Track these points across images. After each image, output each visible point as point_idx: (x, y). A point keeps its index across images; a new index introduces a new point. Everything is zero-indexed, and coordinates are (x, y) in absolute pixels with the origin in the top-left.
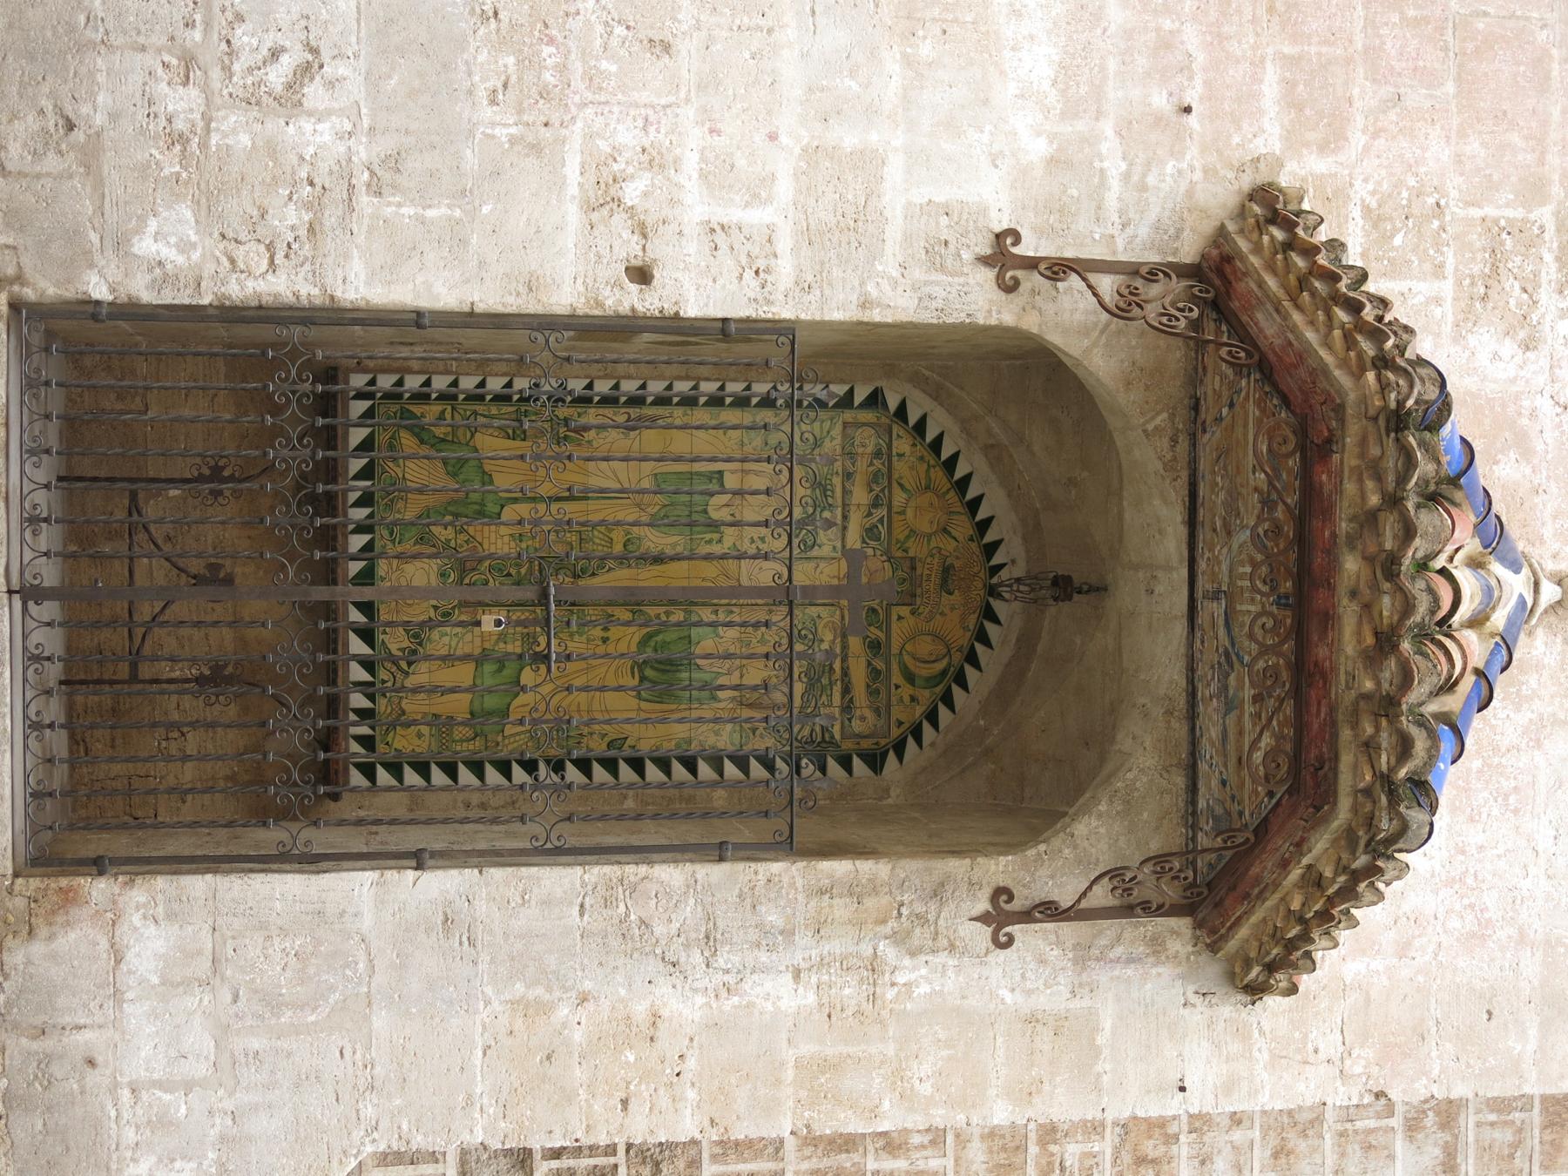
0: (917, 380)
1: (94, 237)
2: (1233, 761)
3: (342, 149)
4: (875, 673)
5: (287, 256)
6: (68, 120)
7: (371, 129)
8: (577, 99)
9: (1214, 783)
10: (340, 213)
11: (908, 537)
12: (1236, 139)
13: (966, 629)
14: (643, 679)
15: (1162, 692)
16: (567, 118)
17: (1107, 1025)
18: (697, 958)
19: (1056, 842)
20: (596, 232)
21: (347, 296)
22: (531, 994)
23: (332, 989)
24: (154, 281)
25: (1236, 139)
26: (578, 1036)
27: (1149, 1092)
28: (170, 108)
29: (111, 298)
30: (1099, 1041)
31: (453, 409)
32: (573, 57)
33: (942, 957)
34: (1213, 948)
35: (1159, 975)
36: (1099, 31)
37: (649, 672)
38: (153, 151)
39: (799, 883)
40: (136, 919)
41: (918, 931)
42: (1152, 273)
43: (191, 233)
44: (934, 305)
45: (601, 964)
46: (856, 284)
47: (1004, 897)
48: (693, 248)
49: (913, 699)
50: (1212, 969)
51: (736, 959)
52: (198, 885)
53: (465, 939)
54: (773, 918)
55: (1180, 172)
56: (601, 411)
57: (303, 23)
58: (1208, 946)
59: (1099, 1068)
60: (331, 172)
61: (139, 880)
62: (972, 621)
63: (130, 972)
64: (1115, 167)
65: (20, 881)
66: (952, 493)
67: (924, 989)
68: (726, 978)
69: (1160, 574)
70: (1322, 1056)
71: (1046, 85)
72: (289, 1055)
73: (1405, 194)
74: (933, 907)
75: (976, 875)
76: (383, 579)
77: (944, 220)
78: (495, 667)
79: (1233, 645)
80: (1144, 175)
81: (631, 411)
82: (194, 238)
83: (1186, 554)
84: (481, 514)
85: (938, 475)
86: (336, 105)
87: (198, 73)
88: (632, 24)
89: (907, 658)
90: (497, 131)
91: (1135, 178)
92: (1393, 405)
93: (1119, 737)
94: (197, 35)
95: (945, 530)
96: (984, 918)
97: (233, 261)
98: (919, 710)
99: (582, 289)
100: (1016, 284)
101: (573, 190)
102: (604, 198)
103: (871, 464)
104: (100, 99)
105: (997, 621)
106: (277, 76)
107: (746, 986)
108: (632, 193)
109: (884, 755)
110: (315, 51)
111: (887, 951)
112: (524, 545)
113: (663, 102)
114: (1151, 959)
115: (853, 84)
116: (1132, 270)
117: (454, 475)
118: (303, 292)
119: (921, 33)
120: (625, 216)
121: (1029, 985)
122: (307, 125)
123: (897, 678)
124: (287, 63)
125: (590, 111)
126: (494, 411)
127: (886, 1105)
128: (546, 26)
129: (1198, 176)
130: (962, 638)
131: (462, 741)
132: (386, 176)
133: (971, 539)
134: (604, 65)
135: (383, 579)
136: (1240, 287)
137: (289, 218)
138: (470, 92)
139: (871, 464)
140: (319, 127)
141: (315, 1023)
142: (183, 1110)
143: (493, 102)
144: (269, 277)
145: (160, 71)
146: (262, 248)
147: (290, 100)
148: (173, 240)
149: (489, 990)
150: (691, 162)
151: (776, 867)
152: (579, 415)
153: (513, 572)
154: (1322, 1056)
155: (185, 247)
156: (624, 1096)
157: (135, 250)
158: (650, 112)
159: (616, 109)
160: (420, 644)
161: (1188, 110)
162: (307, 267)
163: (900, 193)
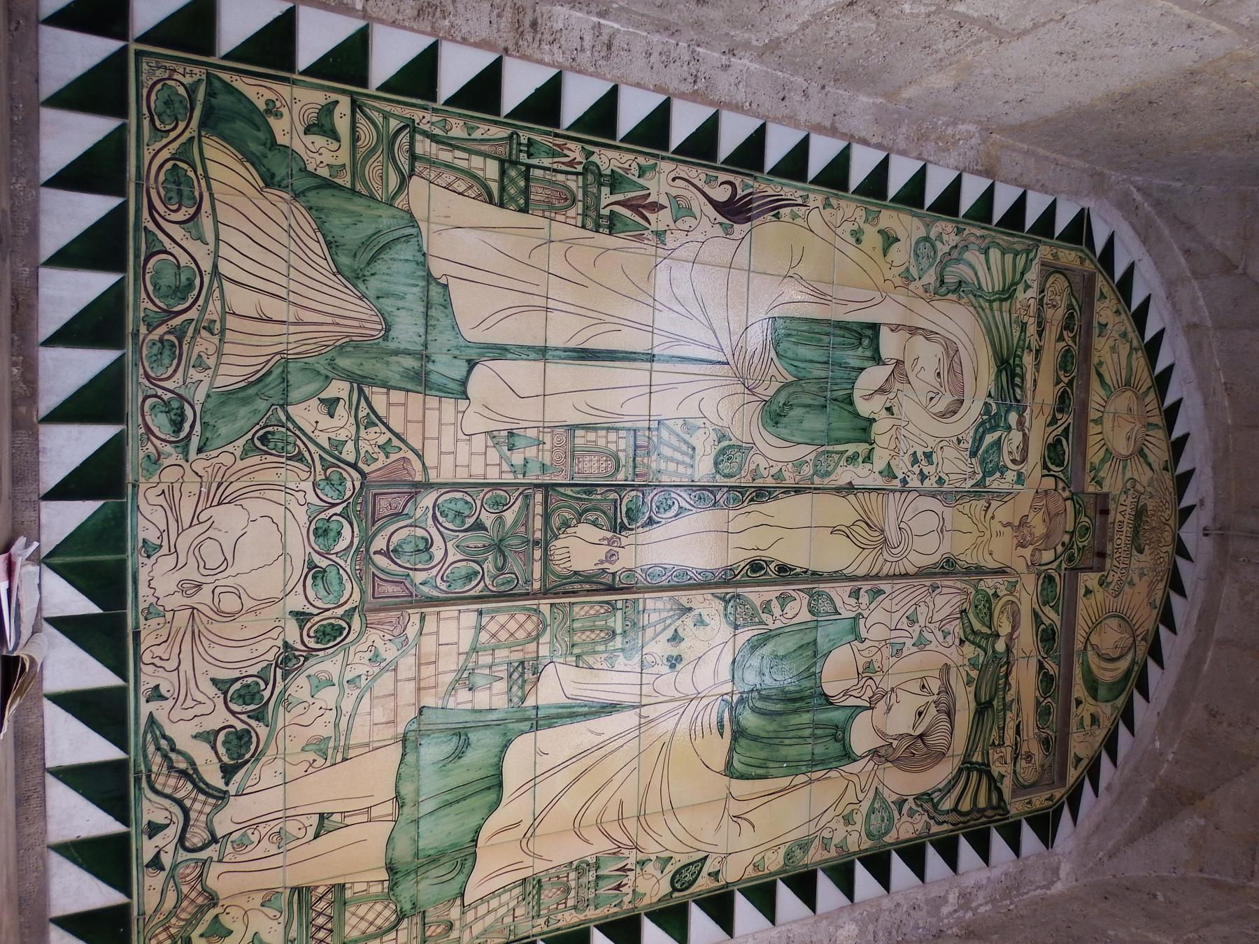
4: (1046, 680)
11: (1103, 461)
13: (1152, 605)
31: (356, 106)
37: (750, 720)
49: (1094, 720)
56: (683, 170)
76: (150, 549)
78: (448, 748)
81: (737, 180)
84: (421, 381)
103: (1061, 338)
112: (517, 458)
117: (356, 278)
126: (457, 130)
133: (1166, 469)
135: (150, 549)
152: (642, 171)
160: (259, 716)
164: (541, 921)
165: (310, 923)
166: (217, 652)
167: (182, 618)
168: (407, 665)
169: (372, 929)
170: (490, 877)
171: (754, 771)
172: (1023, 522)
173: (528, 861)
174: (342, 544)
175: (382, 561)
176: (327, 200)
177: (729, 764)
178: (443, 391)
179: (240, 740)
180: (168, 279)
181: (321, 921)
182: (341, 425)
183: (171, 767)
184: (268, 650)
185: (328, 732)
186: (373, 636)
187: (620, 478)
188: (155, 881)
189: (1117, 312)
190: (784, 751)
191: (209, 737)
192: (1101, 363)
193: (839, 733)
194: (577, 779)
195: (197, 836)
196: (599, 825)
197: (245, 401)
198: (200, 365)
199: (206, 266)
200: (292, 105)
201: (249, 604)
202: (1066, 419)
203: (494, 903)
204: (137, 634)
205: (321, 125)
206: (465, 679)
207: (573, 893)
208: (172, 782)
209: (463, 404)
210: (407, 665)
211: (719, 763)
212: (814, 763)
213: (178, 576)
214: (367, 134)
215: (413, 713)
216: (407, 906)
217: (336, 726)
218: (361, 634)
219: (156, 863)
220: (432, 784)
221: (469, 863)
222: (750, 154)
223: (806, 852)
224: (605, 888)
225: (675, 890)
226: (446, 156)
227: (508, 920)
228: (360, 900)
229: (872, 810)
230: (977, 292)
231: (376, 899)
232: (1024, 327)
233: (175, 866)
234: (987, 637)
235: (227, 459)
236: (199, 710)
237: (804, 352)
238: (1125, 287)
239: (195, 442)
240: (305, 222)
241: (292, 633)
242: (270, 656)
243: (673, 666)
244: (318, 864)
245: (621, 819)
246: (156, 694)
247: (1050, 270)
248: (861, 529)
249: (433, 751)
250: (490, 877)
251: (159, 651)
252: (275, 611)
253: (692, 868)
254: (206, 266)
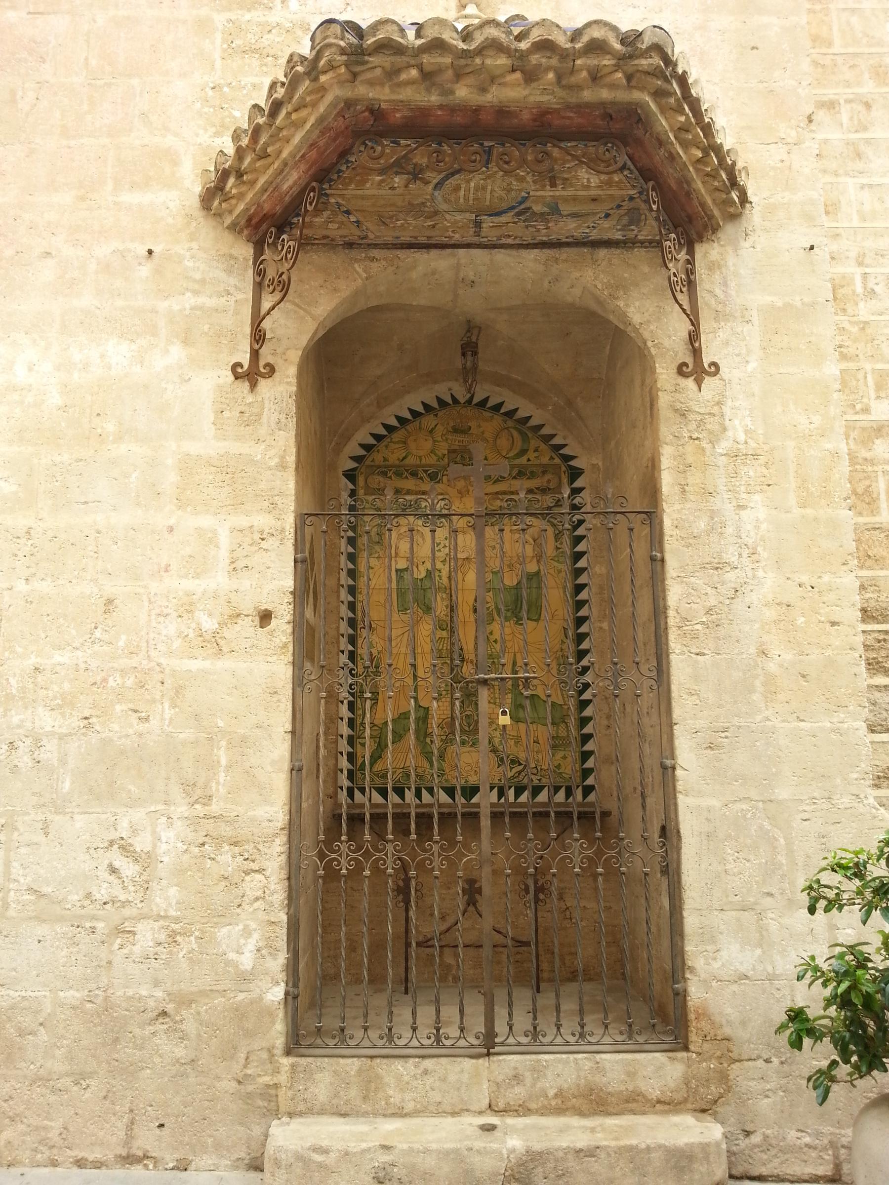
0: (338, 450)
1: (241, 996)
2: (593, 207)
3: (179, 823)
5: (253, 861)
6: (158, 1016)
7: (166, 803)
8: (145, 662)
9: (606, 224)
10: (223, 824)
11: (435, 455)
12: (170, 220)
15: (541, 268)
16: (158, 669)
17: (769, 299)
18: (731, 576)
19: (646, 335)
20: (237, 648)
21: (281, 819)
22: (760, 688)
23: (761, 827)
24: (270, 954)
25: (170, 220)
26: (788, 656)
27: (813, 271)
28: (151, 944)
29: (283, 984)
30: (780, 304)
32: (115, 665)
33: (727, 410)
34: (715, 229)
35: (734, 265)
36: (98, 311)
38: (181, 955)
39: (677, 507)
40: (716, 965)
41: (709, 426)
42: (260, 273)
43: (237, 928)
44: (283, 420)
45: (737, 641)
46: (269, 472)
47: (684, 369)
48: (246, 583)
49: (536, 450)
50: (729, 230)
51: (731, 549)
52: (691, 921)
53: (723, 735)
54: (702, 525)
55: (192, 257)
56: (359, 645)
57: (92, 851)
58: (713, 233)
59: (798, 304)
60: (195, 831)
61: (689, 963)
62: (487, 414)
63: (754, 969)
64: (190, 300)
65: (692, 1047)
66: (408, 427)
67: (748, 421)
68: (745, 555)
69: (462, 275)
70: (785, 157)
71: (134, 347)
72: (808, 857)
73: (206, 110)
74: (691, 416)
75: (669, 387)
76: (467, 781)
77: (226, 414)
78: (521, 710)
79: (513, 208)
80: (195, 281)
81: (359, 627)
82: (241, 927)
83: (449, 251)
85: (397, 436)
86: (149, 828)
87: (126, 924)
88: (93, 625)
89: (511, 454)
90: (167, 716)
91: (196, 287)
92: (345, 58)
93: (569, 299)
94: (100, 925)
95: (431, 432)
96: (699, 383)
97: (257, 899)
98: (543, 446)
99: (275, 657)
100: (268, 365)
101: (207, 664)
102: (214, 644)
103: (390, 478)
104: (144, 993)
105: (487, 399)
106: (129, 869)
107: (750, 542)
108: (209, 624)
109: (571, 468)
110: (112, 843)
111: (723, 446)
112: (444, 693)
113: (146, 604)
114: (724, 270)
115: (134, 476)
116: (259, 287)
118: (279, 849)
119: (99, 431)
120: (225, 629)
121: (744, 351)
122: (164, 847)
123: (523, 460)
124: (120, 862)
125: (153, 653)
126: (360, 712)
127: (828, 446)
128: (95, 683)
129: (194, 245)
130: (498, 420)
132: (199, 792)
134: (121, 644)
135: (467, 781)
136: (267, 207)
137: (228, 861)
138: (141, 735)
139: (390, 478)
140: (164, 839)
141: (785, 838)
142: (849, 931)
143: (147, 719)
144: (267, 873)
145: (125, 951)
146: (248, 878)
147: (146, 860)
148: (242, 941)
149: (759, 718)
150: (190, 584)
151: (667, 522)
152: (362, 659)
154: (785, 157)
155: (247, 933)
156: (829, 625)
157: (249, 968)
158: (153, 612)
159: (152, 635)
161: (150, 252)
162: (260, 847)
163: (208, 444)
172: (460, 492)
177: (535, 620)
179: (513, 762)
180: (405, 778)
187: (449, 662)
188: (544, 781)
189: (378, 451)
191: (511, 768)
192: (398, 459)
193: (531, 577)
195: (535, 771)
198: (424, 771)
202: (421, 474)
219: (539, 780)
228: (557, 732)
229: (558, 561)
231: (558, 729)
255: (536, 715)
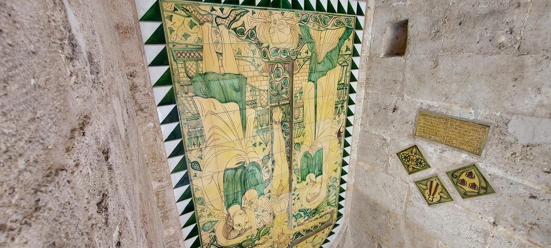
14: (236, 169)
37: (240, 171)
56: (344, 120)
76: (282, 13)
78: (236, 86)
84: (311, 72)
112: (298, 95)
117: (327, 56)
131: (185, 68)
135: (282, 13)
153: (284, 90)
160: (247, 37)
164: (185, 122)
165: (192, 51)
166: (262, 27)
167: (269, 20)
168: (257, 73)
169: (188, 70)
170: (201, 103)
171: (226, 177)
173: (204, 114)
174: (282, 56)
175: (276, 66)
176: (338, 50)
178: (309, 76)
179: (242, 33)
180: (326, 20)
181: (192, 54)
182: (304, 55)
183: (237, 15)
184: (261, 40)
185: (243, 55)
186: (264, 64)
187: (294, 120)
190: (231, 186)
191: (243, 25)
193: (235, 201)
194: (226, 124)
195: (219, 21)
196: (214, 134)
197: (308, 35)
198: (314, 26)
199: (328, 27)
200: (349, 43)
201: (271, 35)
202: (304, 234)
203: (192, 106)
204: (266, 9)
205: (348, 49)
206: (253, 89)
207: (193, 130)
208: (233, 15)
209: (307, 81)
210: (257, 73)
211: (229, 167)
212: (227, 196)
213: (277, 19)
214: (346, 57)
215: (246, 76)
216: (194, 80)
217: (244, 57)
218: (264, 61)
219: (213, 10)
220: (227, 83)
221: (205, 96)
222: (347, 134)
223: (201, 204)
224: (194, 140)
225: (192, 163)
226: (344, 72)
227: (187, 111)
230: (328, 196)
232: (323, 211)
233: (211, 14)
234: (259, 237)
235: (298, 31)
236: (250, 23)
237: (317, 157)
238: (331, 233)
239: (301, 24)
240: (334, 46)
241: (265, 45)
242: (260, 40)
243: (254, 145)
244: (209, 53)
245: (215, 140)
246: (254, 13)
247: (332, 213)
248: (281, 188)
249: (236, 82)
250: (201, 103)
251: (263, 14)
252: (270, 41)
253: (198, 167)
254: (328, 27)
255: (222, 82)
